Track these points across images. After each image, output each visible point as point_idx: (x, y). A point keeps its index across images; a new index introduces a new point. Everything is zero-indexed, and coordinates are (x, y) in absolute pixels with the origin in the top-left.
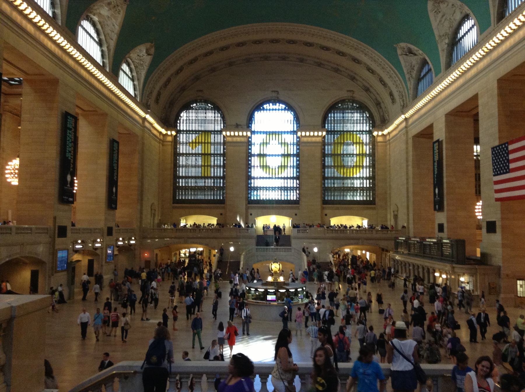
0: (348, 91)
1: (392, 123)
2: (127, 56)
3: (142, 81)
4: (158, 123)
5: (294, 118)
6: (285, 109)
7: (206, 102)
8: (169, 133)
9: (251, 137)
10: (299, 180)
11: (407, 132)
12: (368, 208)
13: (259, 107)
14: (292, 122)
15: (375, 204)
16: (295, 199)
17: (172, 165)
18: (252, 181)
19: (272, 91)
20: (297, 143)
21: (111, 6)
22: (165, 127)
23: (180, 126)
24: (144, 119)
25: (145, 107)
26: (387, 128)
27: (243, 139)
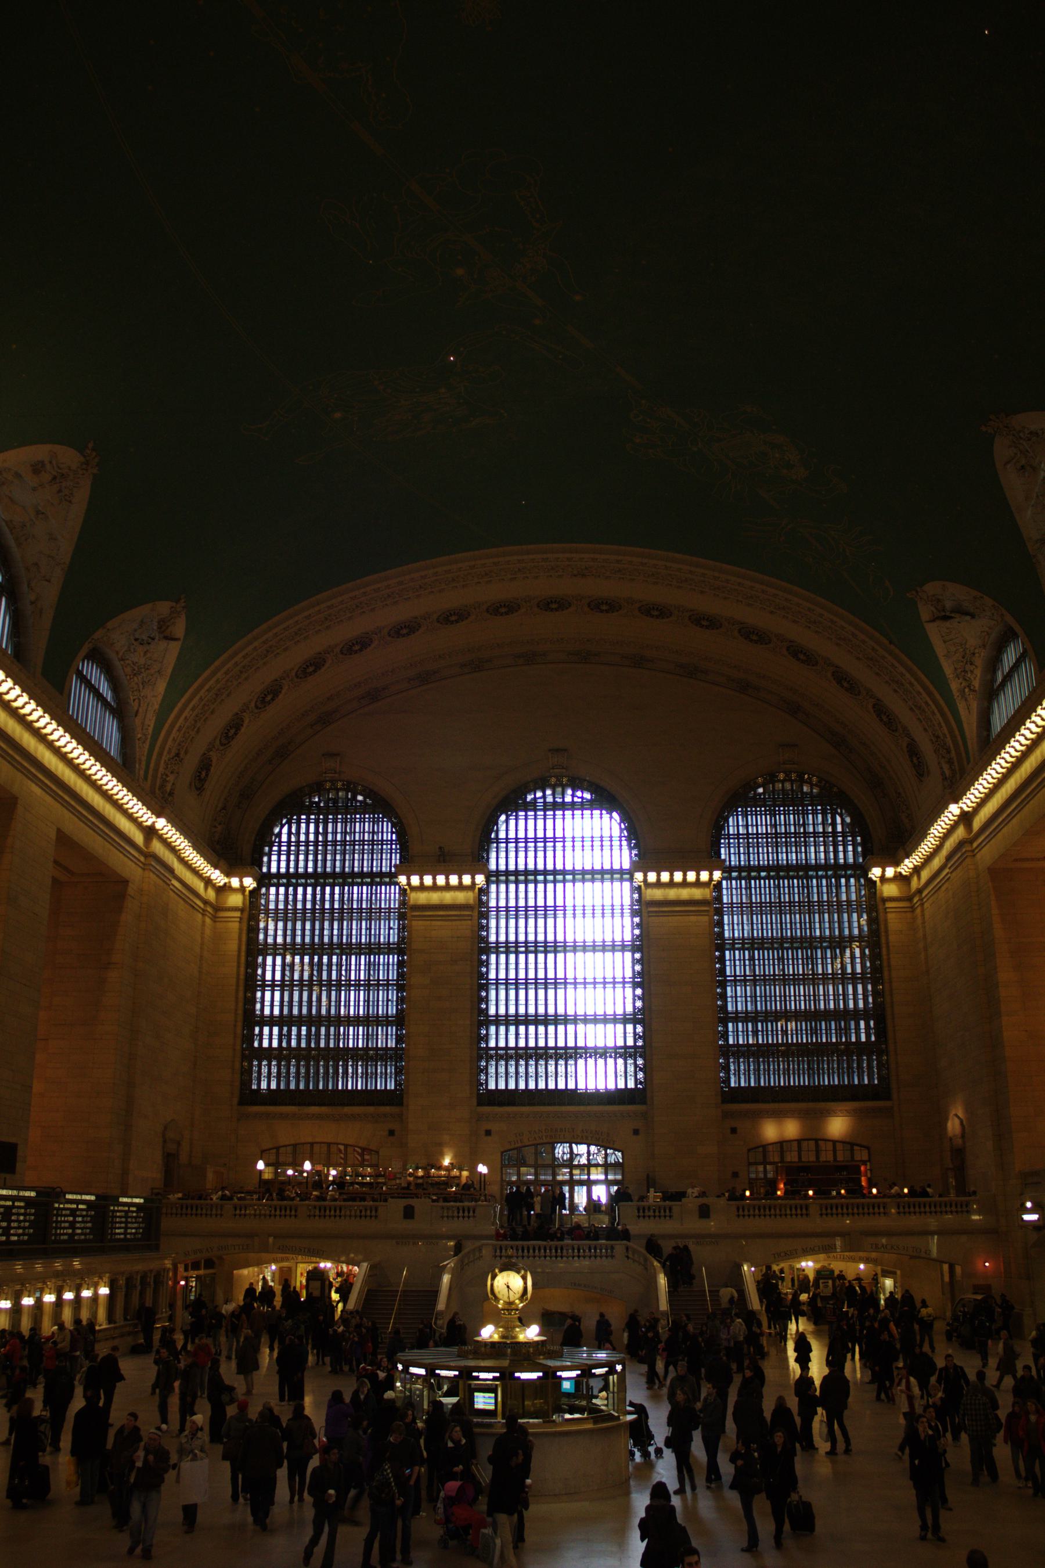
1: (924, 835)
4: (196, 847)
5: (621, 830)
6: (591, 805)
7: (351, 787)
8: (235, 882)
9: (484, 891)
13: (514, 802)
14: (616, 843)
15: (888, 1098)
16: (631, 1085)
18: (493, 1029)
20: (632, 905)
22: (222, 863)
23: (270, 861)
27: (461, 897)
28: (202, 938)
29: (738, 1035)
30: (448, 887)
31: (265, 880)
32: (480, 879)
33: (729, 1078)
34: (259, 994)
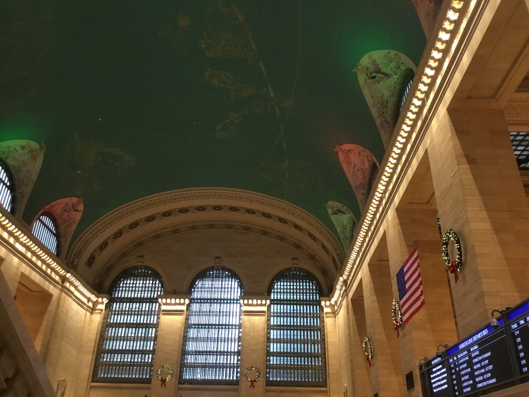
0: (293, 259)
1: (336, 289)
2: (48, 207)
3: (69, 238)
8: (100, 300)
10: (240, 355)
11: (347, 295)
12: (317, 392)
14: (236, 290)
17: (98, 336)
19: (215, 258)
21: (26, 151)
22: (95, 292)
24: (64, 279)
25: (70, 265)
26: (333, 297)
28: (85, 319)
29: (273, 361)
30: (175, 304)
31: (112, 301)
32: (187, 301)
33: (269, 377)
34: (105, 342)
